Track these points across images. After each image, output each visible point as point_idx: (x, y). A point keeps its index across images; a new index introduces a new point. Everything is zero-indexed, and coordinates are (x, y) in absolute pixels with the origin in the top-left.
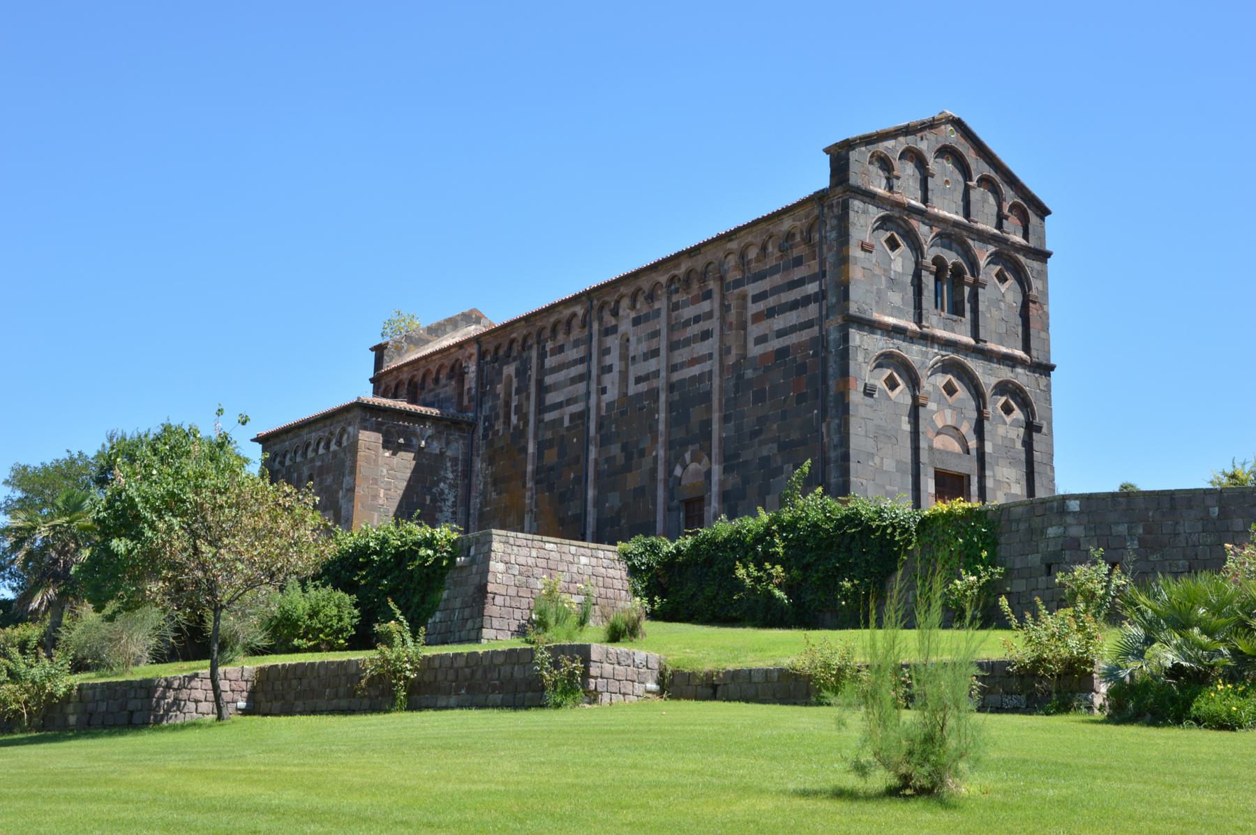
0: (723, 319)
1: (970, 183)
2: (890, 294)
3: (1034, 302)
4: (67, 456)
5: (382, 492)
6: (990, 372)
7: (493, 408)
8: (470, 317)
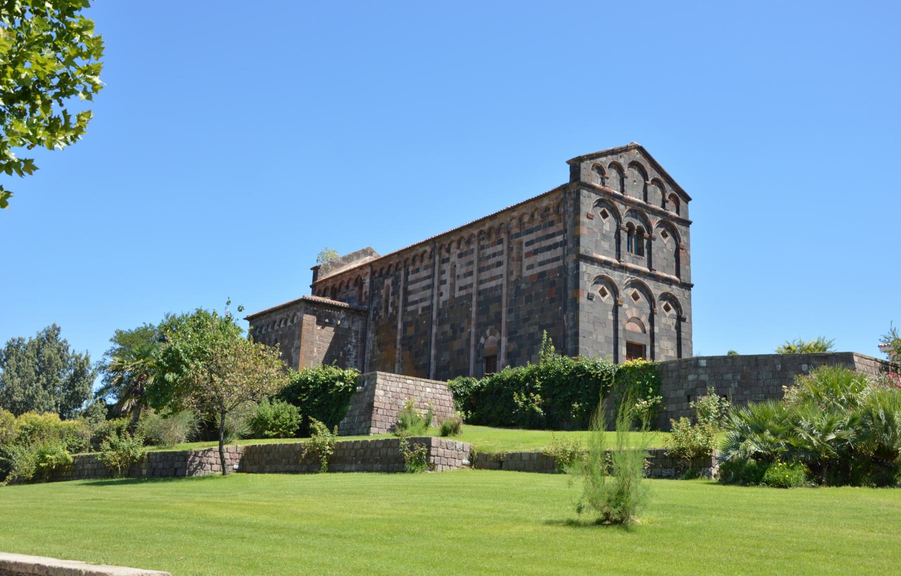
0: (509, 255)
1: (647, 182)
2: (602, 242)
3: (682, 249)
4: (143, 326)
5: (316, 349)
7: (379, 303)
8: (366, 252)
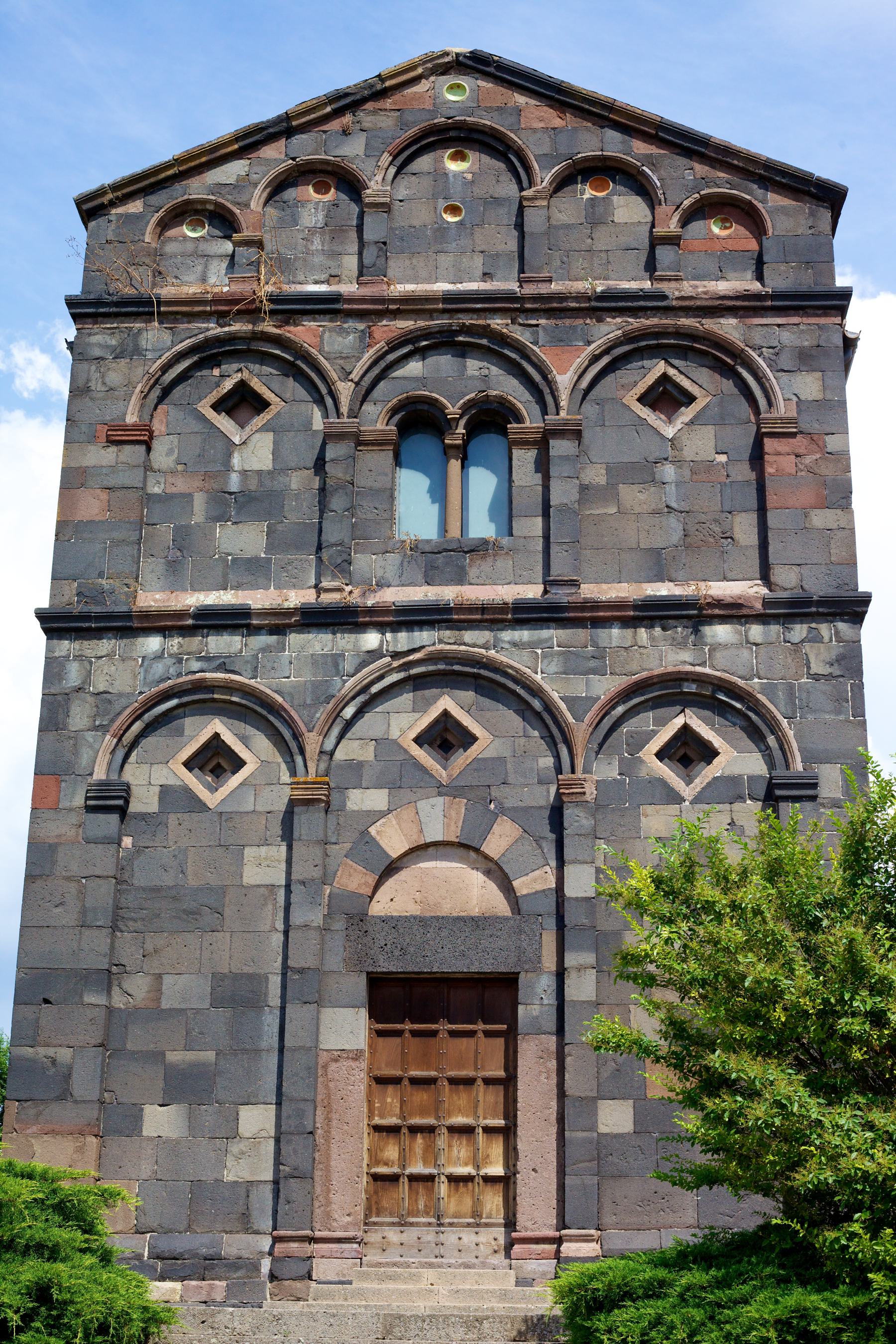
6: (592, 664)
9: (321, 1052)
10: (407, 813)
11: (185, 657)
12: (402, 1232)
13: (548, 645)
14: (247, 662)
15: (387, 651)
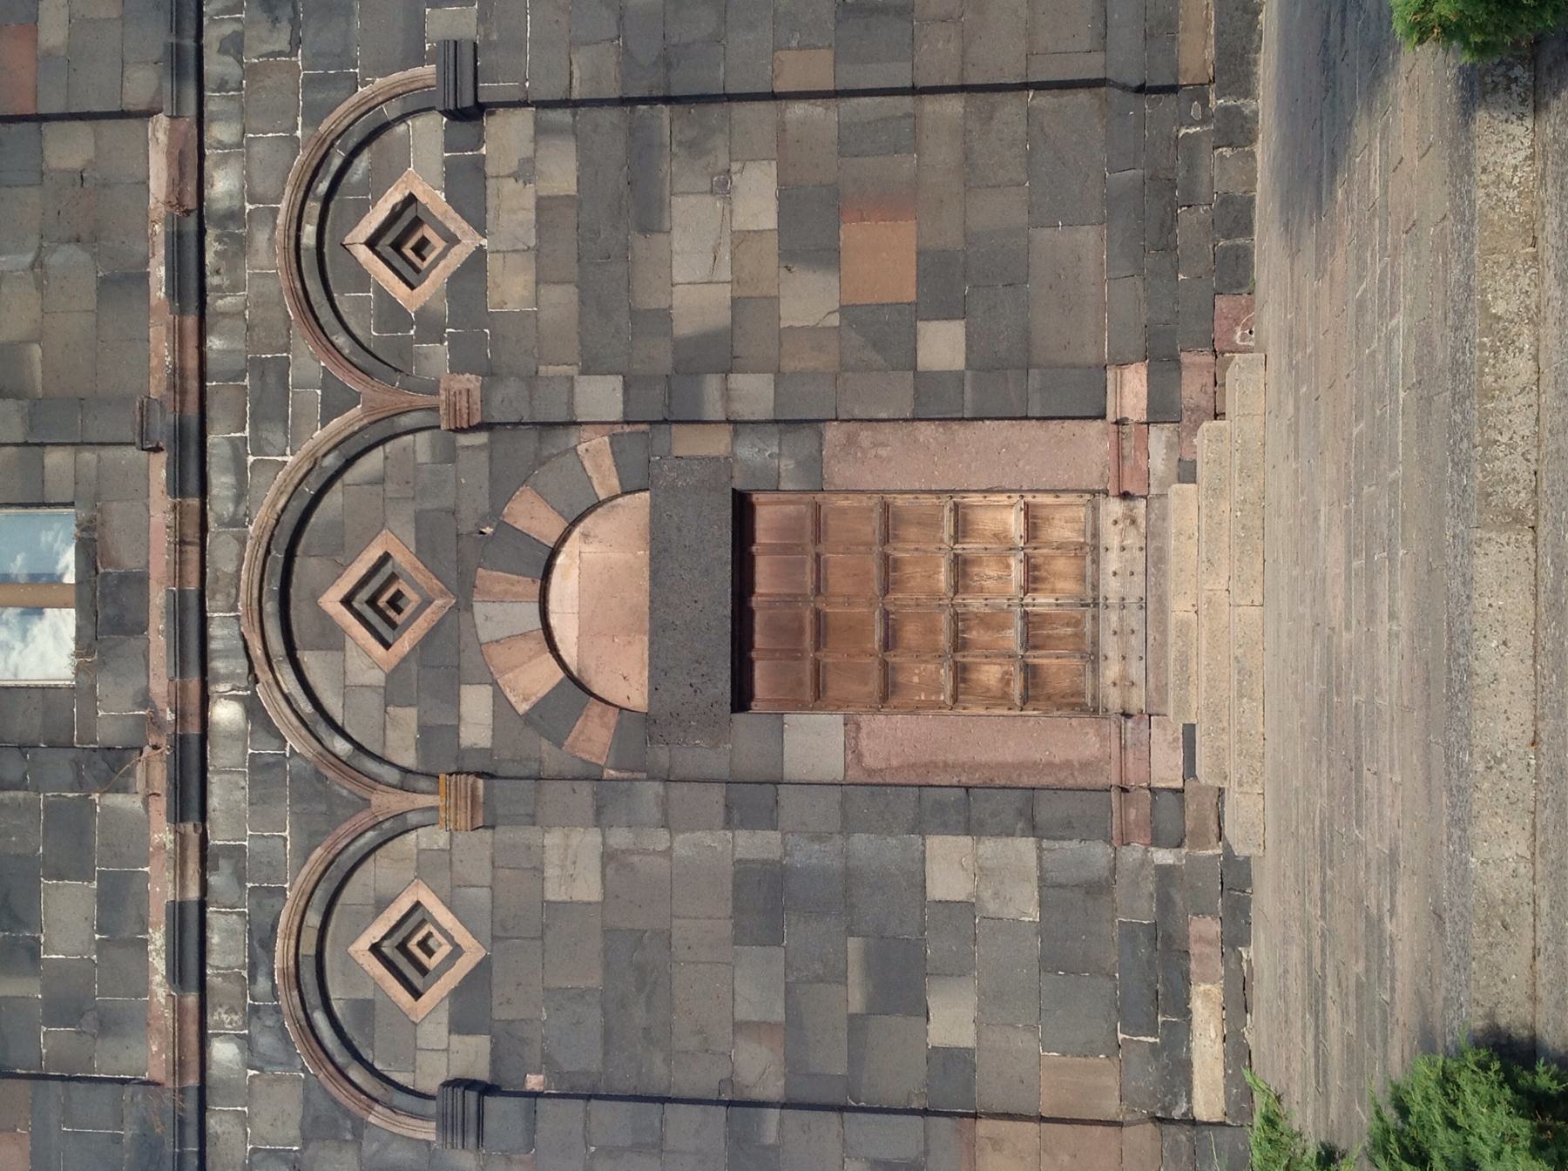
9: (848, 778)
10: (498, 657)
11: (249, 1001)
12: (1106, 658)
13: (240, 445)
14: (259, 904)
15: (246, 689)
